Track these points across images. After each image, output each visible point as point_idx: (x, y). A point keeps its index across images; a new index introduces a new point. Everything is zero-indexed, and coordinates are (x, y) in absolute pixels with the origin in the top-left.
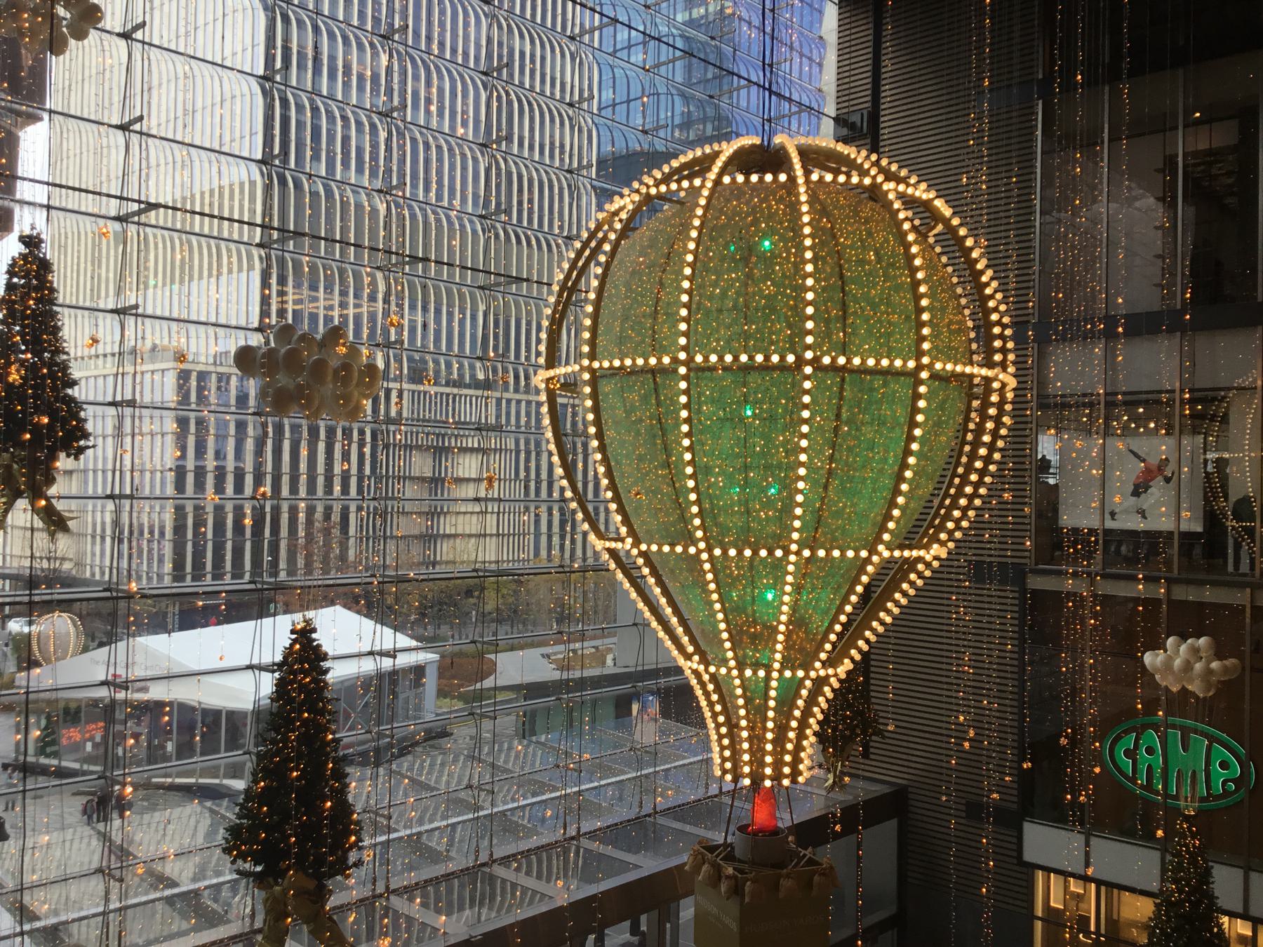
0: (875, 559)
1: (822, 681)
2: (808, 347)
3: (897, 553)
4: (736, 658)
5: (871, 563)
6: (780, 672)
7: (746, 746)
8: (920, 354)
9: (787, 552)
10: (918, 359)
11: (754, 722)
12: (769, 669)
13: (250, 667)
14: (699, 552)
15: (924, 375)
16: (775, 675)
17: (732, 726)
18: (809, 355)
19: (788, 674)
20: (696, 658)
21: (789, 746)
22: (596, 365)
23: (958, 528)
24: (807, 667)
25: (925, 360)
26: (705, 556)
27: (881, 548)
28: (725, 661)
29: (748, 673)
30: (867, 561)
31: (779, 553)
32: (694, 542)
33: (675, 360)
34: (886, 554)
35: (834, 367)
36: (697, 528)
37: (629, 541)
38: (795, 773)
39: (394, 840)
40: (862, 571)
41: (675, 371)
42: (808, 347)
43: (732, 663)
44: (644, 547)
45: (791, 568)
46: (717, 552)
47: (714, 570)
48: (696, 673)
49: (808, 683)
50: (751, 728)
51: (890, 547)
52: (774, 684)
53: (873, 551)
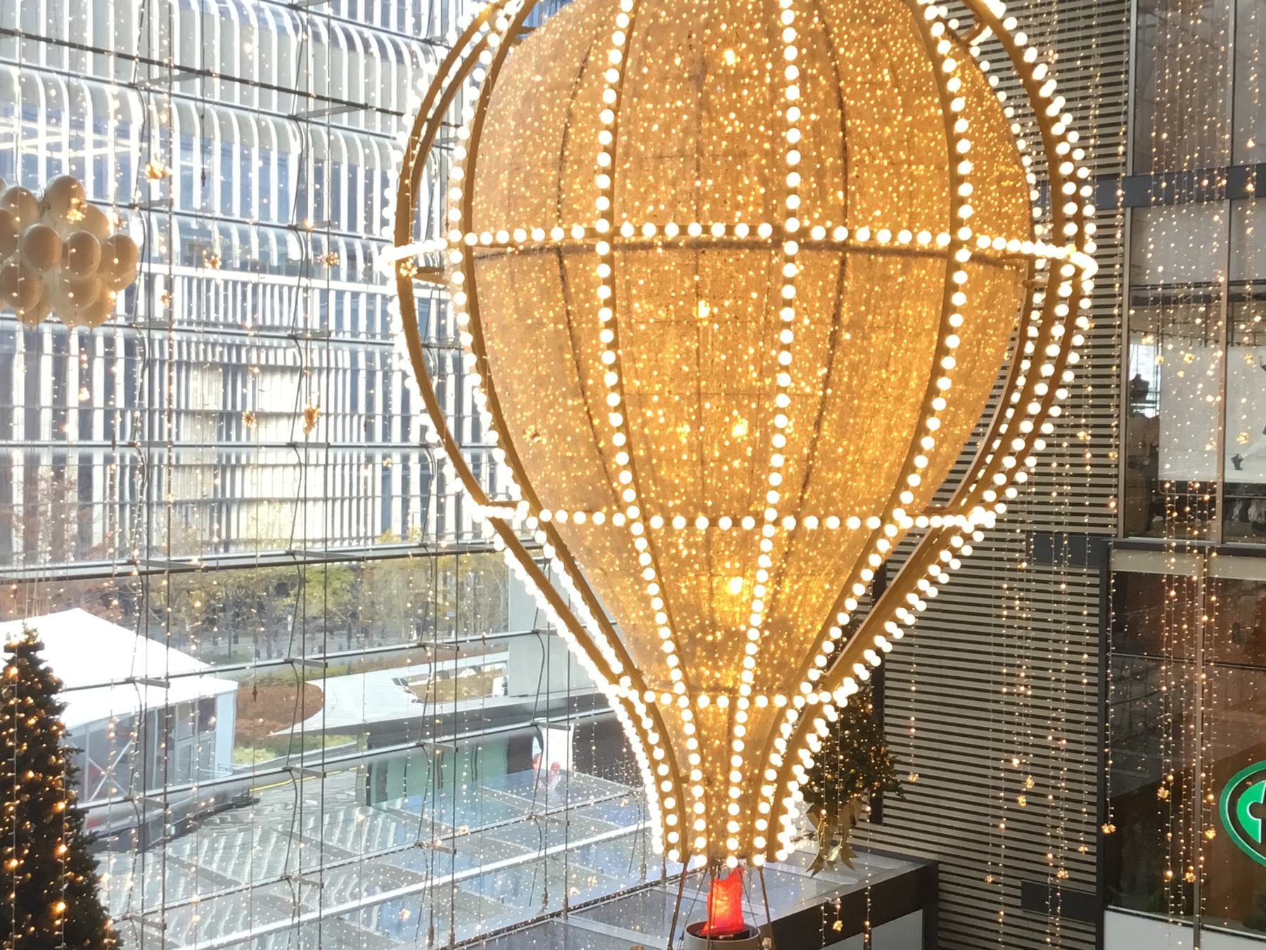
0: (890, 530)
2: (791, 214)
3: (922, 522)
4: (686, 679)
6: (751, 699)
7: (700, 808)
9: (760, 521)
13: (130, 681)
15: (963, 255)
16: (743, 703)
17: (680, 780)
18: (792, 225)
19: (761, 701)
20: (626, 681)
21: (764, 808)
22: (471, 239)
23: (1011, 483)
24: (790, 689)
25: (964, 233)
26: (637, 529)
28: (668, 684)
30: (878, 533)
31: (748, 523)
33: (592, 233)
35: (829, 245)
37: (524, 506)
38: (772, 847)
39: (327, 917)
40: (870, 547)
41: (591, 249)
42: (791, 214)
43: (680, 688)
44: (546, 515)
45: (766, 546)
47: (653, 549)
48: (626, 703)
49: (792, 715)
50: (709, 781)
51: (911, 514)
52: (741, 717)
53: (886, 518)
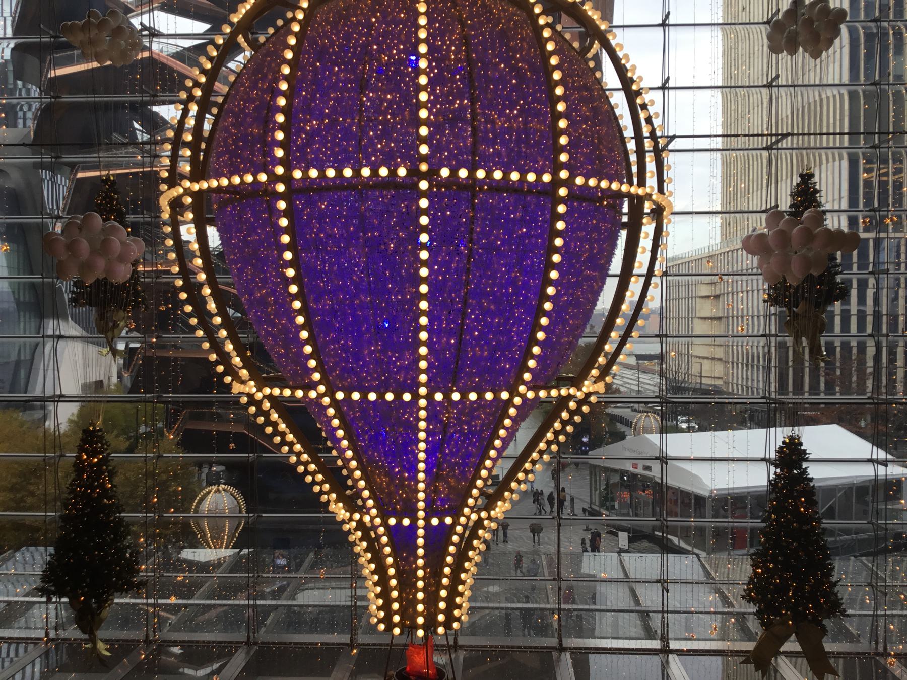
0: (517, 401)
2: (424, 158)
6: (427, 519)
8: (556, 167)
9: (416, 397)
10: (555, 174)
12: (414, 519)
14: (320, 396)
15: (563, 192)
16: (421, 523)
18: (424, 167)
19: (435, 522)
24: (456, 513)
25: (564, 174)
27: (522, 389)
30: (509, 403)
32: (313, 386)
34: (530, 395)
43: (374, 512)
47: (339, 414)
50: (398, 575)
51: (534, 387)
52: (421, 532)
53: (514, 393)
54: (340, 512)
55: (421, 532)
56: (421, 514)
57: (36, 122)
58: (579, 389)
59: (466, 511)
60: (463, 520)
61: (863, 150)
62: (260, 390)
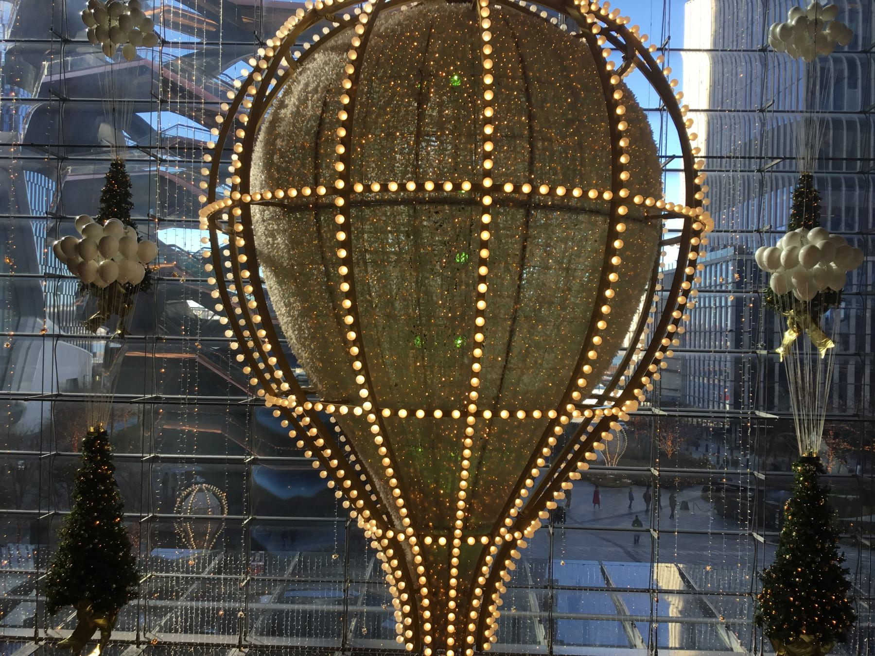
0: (564, 419)
1: (513, 544)
5: (559, 424)
6: (463, 539)
7: (427, 614)
9: (465, 414)
11: (438, 588)
12: (450, 538)
14: (365, 414)
15: (622, 211)
16: (457, 542)
19: (471, 541)
25: (623, 193)
29: (428, 540)
30: (556, 422)
31: (456, 414)
32: (360, 402)
36: (362, 386)
40: (549, 432)
46: (386, 413)
47: (383, 432)
52: (456, 551)
53: (561, 411)
54: (372, 529)
55: (456, 551)
56: (458, 532)
57: (27, 126)
58: (621, 410)
59: (502, 530)
60: (498, 539)
61: (844, 175)
62: (300, 403)
